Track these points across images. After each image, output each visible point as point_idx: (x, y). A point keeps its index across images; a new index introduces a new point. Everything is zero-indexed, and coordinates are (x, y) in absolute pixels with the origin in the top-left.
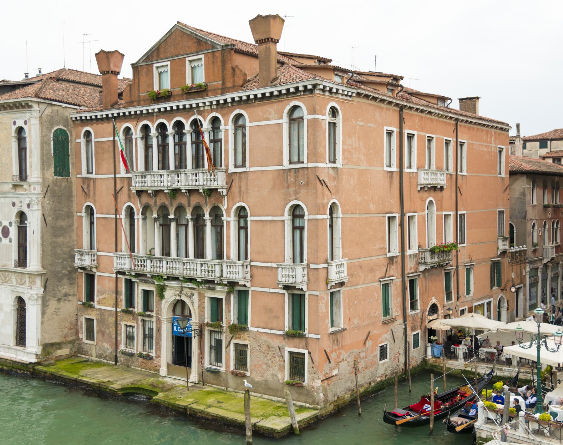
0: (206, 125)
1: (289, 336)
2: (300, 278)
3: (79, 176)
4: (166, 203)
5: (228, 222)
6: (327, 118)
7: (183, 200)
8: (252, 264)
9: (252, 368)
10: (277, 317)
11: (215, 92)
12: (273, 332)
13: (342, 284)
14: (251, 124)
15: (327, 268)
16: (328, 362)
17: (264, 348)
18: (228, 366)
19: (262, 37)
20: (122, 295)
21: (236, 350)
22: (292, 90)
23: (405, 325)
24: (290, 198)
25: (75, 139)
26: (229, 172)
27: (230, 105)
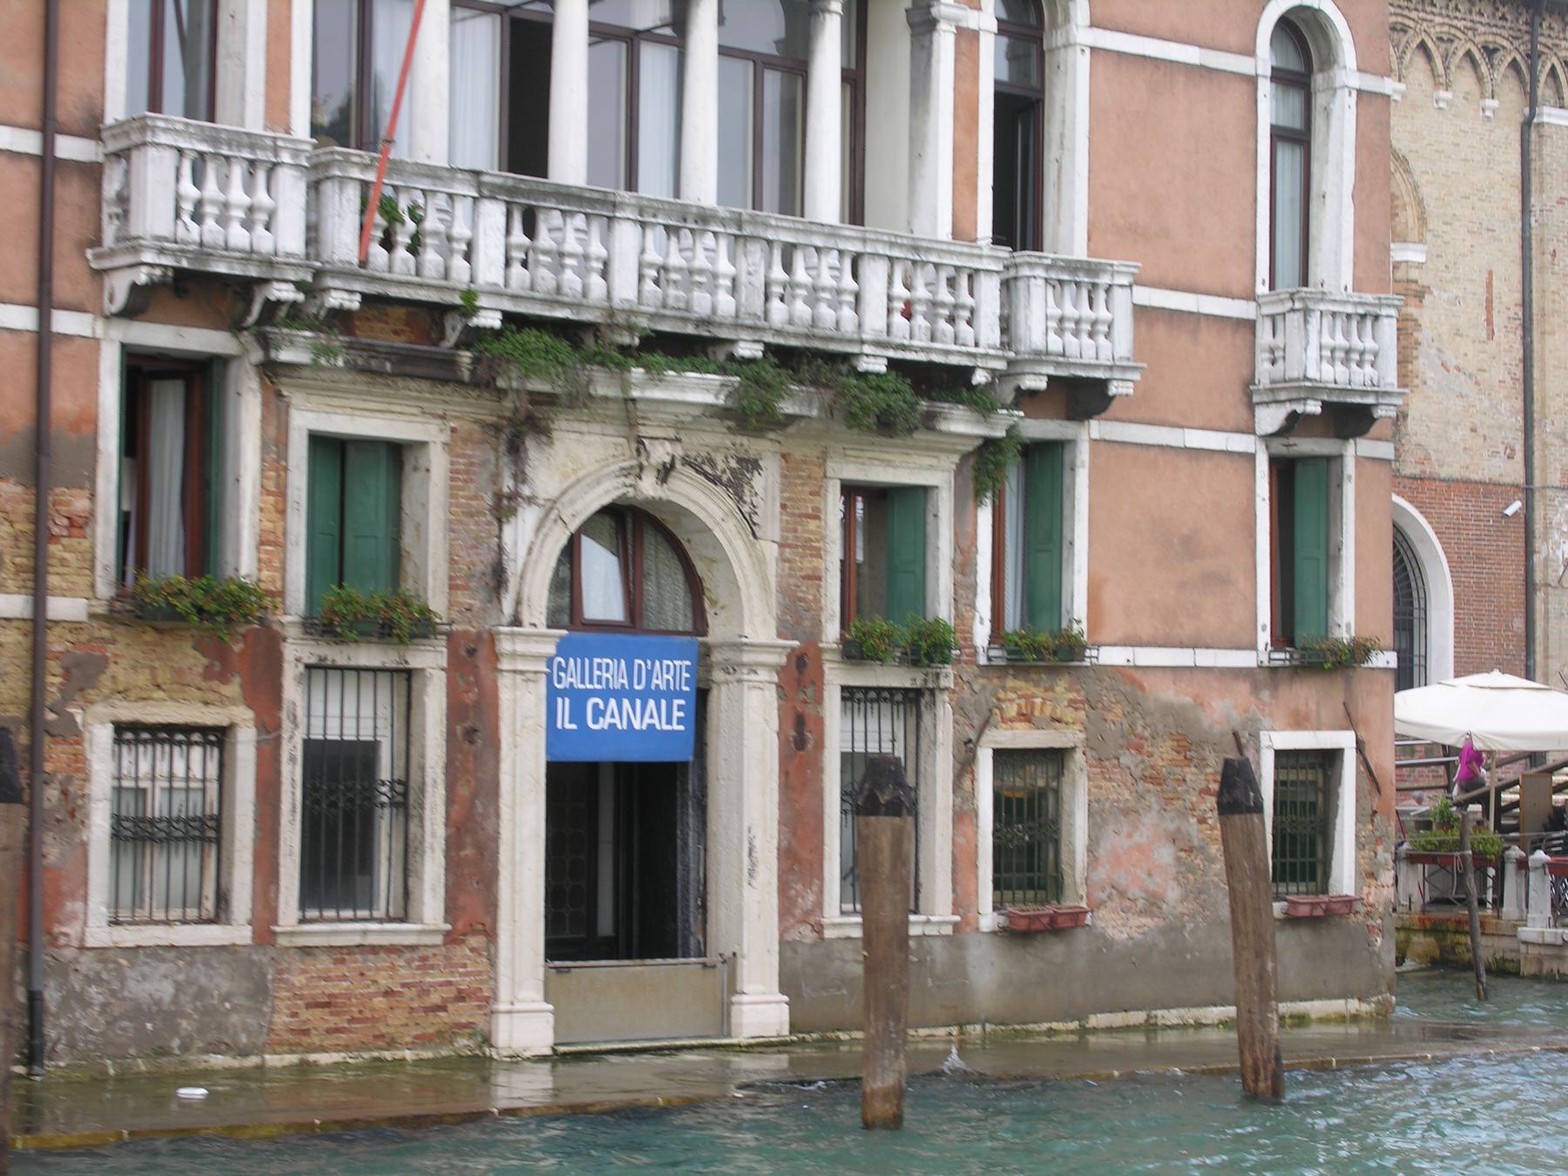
10: (1217, 581)
12: (1206, 658)
20: (87, 482)
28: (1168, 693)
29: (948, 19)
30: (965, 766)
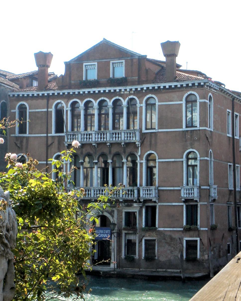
0: (124, 103)
1: (186, 230)
2: (195, 195)
3: (12, 135)
4: (91, 152)
5: (141, 164)
6: (208, 101)
7: (106, 151)
8: (159, 188)
9: (159, 253)
11: (133, 84)
12: (175, 229)
13: (214, 200)
14: (160, 104)
15: (209, 189)
16: (210, 246)
17: (169, 240)
18: (140, 255)
19: (169, 53)
21: (146, 244)
22: (190, 85)
23: (237, 234)
24: (187, 148)
25: (10, 110)
26: (143, 132)
27: (144, 91)
28: (169, 234)
29: (139, 162)
30: (140, 241)
